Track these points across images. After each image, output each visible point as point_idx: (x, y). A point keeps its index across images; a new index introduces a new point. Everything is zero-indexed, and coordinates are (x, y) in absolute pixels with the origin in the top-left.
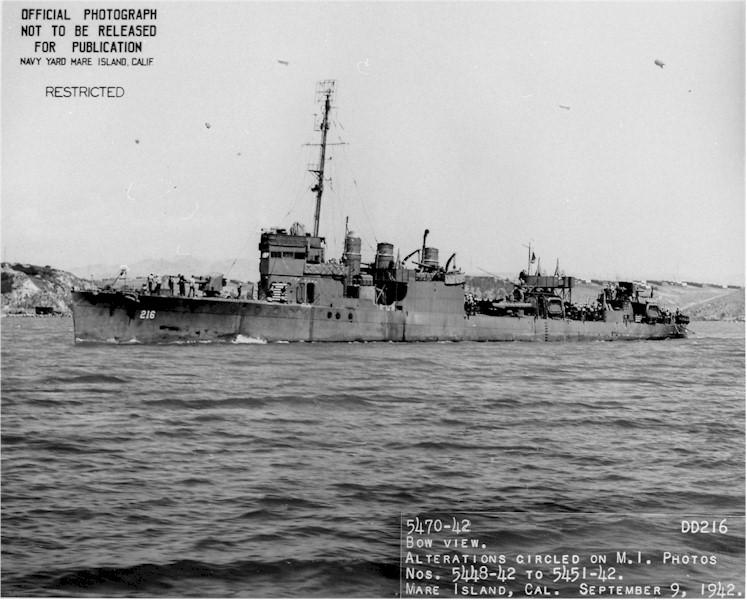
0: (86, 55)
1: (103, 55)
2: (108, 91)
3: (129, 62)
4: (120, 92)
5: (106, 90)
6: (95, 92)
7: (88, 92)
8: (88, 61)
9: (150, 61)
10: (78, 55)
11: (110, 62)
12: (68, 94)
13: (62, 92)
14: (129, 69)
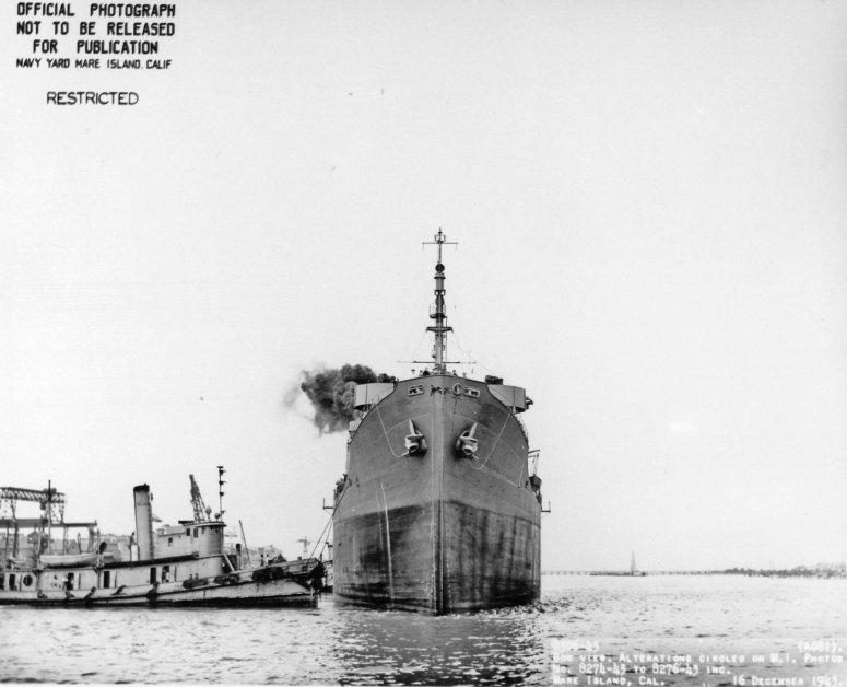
0: (92, 56)
1: (112, 56)
2: (120, 98)
3: (143, 64)
4: (133, 99)
5: (116, 96)
6: (104, 98)
7: (96, 99)
8: (95, 63)
9: (167, 63)
10: (83, 56)
11: (121, 64)
12: (72, 101)
13: (65, 99)
14: (143, 72)
